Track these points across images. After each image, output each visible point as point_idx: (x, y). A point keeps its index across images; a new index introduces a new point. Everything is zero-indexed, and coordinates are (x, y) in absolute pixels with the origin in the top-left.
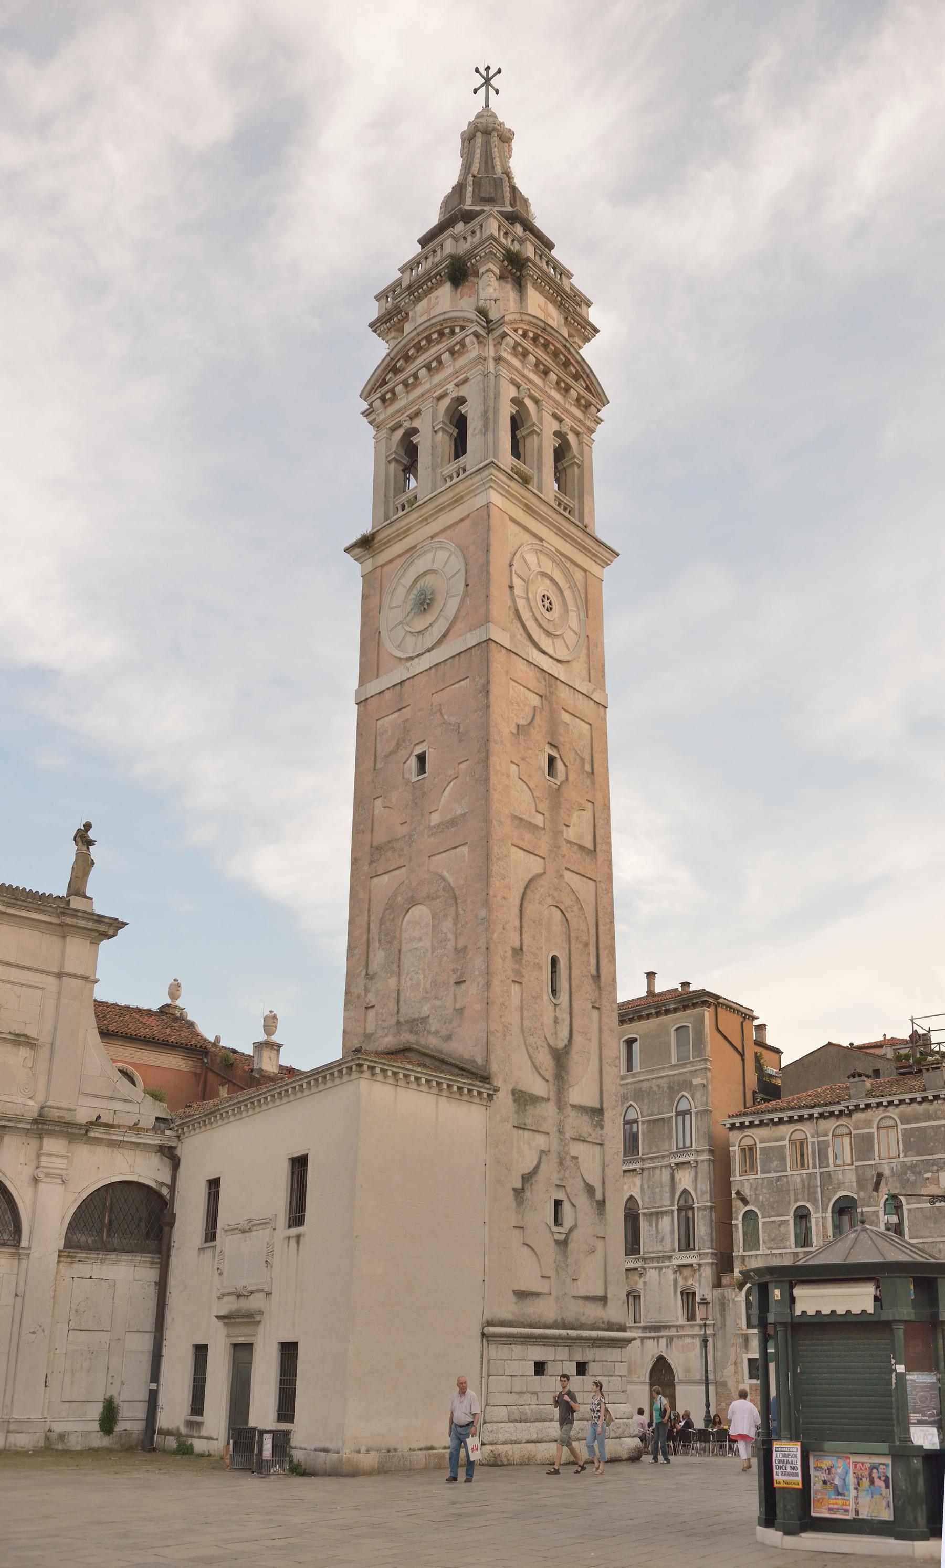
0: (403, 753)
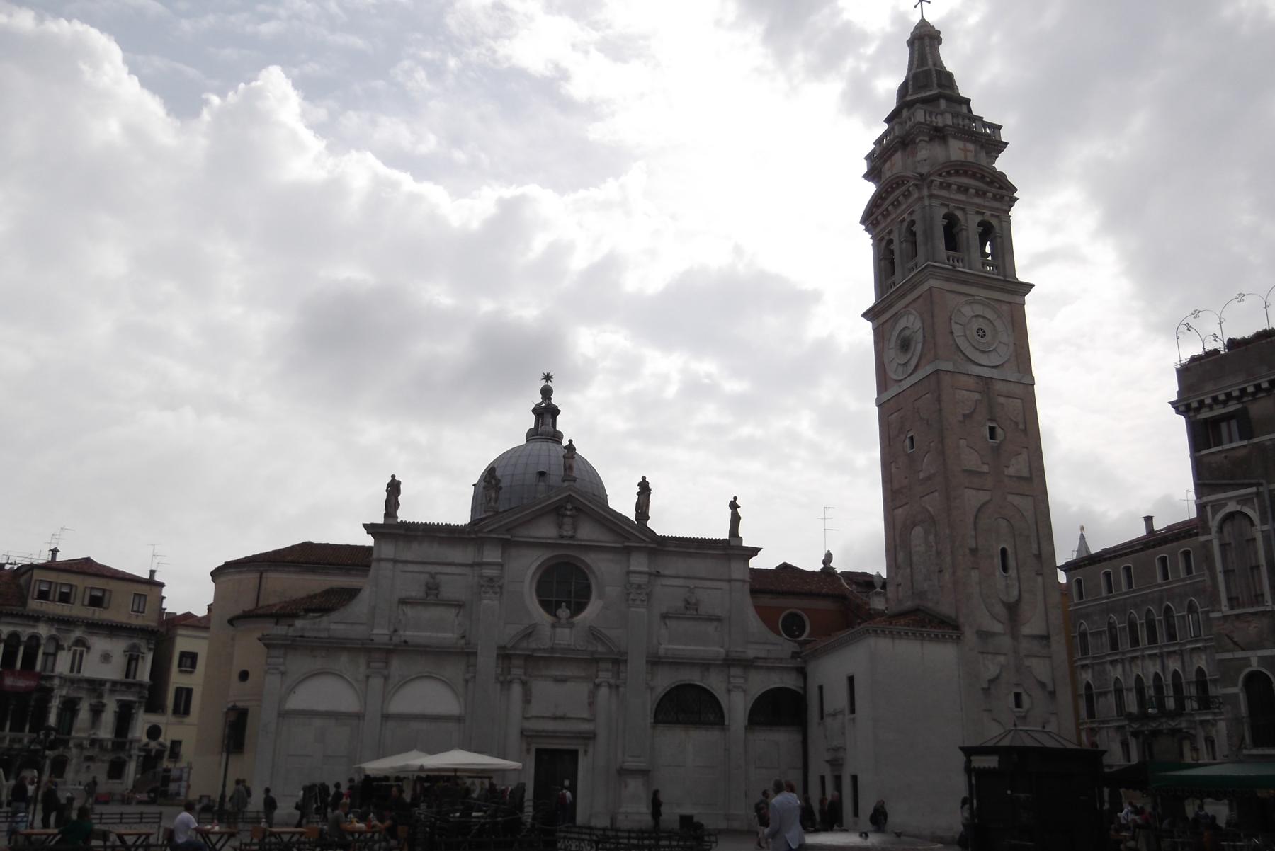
0: (903, 436)
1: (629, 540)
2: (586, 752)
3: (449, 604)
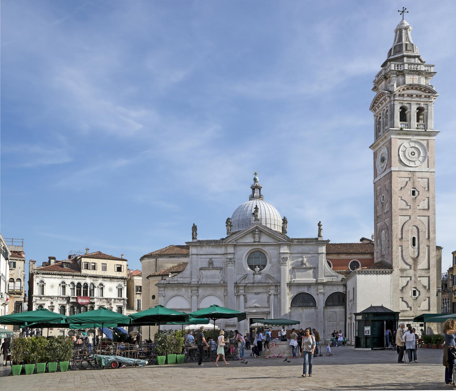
1: (279, 241)
3: (216, 268)
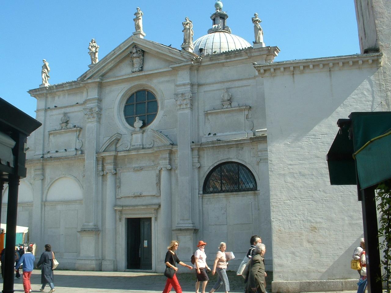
2: (156, 219)
